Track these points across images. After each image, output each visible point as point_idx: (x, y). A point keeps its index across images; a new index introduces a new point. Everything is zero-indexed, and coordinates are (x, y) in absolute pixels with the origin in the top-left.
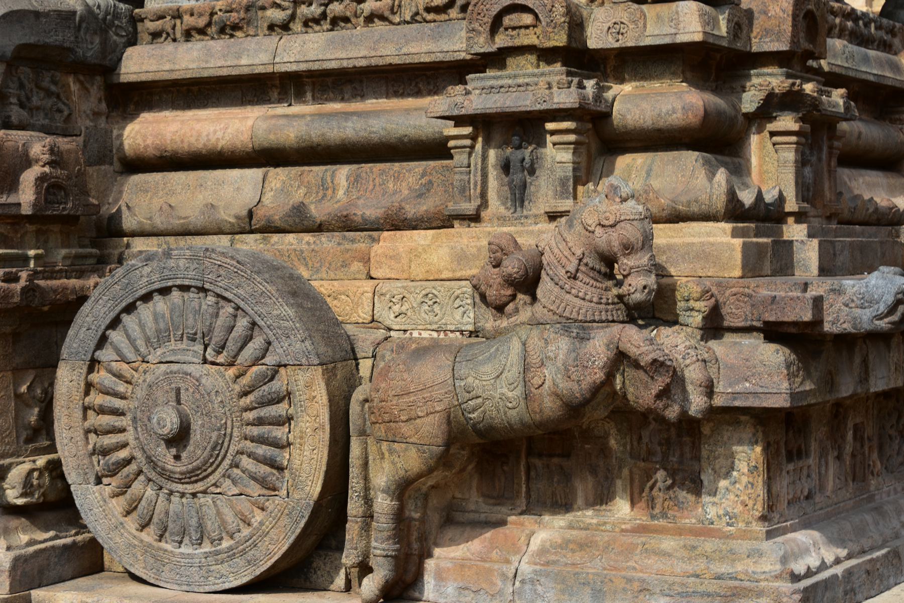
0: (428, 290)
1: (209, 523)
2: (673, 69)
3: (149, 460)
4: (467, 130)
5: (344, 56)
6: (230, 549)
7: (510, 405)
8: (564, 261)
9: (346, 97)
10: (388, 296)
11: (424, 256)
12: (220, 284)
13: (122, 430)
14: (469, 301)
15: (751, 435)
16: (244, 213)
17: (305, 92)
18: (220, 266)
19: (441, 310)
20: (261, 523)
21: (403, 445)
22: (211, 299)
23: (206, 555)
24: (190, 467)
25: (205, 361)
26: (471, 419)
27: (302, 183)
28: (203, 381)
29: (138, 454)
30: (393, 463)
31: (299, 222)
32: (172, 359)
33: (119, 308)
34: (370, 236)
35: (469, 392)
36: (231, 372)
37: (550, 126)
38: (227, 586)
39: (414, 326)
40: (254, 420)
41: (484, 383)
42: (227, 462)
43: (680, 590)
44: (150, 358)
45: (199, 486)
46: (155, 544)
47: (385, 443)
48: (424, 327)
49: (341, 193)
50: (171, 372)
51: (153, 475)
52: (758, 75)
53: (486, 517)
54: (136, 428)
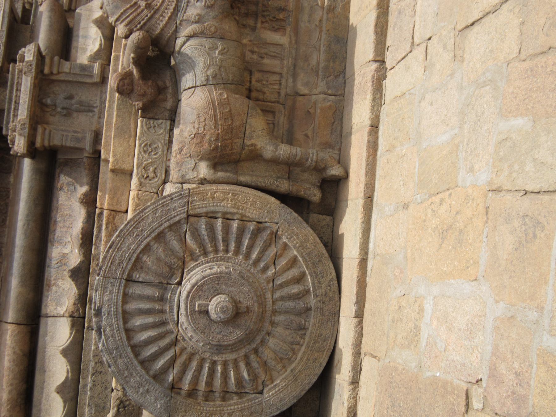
0: (142, 150)
1: (293, 291)
3: (248, 339)
4: (40, 130)
8: (139, 10)
10: (142, 180)
13: (225, 364)
14: (152, 122)
16: (70, 319)
18: (111, 263)
19: (155, 143)
21: (248, 127)
23: (316, 296)
25: (180, 283)
26: (233, 80)
27: (54, 284)
28: (193, 281)
29: (242, 352)
30: (258, 137)
31: (81, 275)
37: (46, 70)
38: (336, 282)
39: (164, 164)
44: (173, 336)
45: (269, 296)
47: (245, 141)
48: (165, 157)
49: (66, 251)
50: (186, 309)
51: (259, 339)
52: (35, 16)
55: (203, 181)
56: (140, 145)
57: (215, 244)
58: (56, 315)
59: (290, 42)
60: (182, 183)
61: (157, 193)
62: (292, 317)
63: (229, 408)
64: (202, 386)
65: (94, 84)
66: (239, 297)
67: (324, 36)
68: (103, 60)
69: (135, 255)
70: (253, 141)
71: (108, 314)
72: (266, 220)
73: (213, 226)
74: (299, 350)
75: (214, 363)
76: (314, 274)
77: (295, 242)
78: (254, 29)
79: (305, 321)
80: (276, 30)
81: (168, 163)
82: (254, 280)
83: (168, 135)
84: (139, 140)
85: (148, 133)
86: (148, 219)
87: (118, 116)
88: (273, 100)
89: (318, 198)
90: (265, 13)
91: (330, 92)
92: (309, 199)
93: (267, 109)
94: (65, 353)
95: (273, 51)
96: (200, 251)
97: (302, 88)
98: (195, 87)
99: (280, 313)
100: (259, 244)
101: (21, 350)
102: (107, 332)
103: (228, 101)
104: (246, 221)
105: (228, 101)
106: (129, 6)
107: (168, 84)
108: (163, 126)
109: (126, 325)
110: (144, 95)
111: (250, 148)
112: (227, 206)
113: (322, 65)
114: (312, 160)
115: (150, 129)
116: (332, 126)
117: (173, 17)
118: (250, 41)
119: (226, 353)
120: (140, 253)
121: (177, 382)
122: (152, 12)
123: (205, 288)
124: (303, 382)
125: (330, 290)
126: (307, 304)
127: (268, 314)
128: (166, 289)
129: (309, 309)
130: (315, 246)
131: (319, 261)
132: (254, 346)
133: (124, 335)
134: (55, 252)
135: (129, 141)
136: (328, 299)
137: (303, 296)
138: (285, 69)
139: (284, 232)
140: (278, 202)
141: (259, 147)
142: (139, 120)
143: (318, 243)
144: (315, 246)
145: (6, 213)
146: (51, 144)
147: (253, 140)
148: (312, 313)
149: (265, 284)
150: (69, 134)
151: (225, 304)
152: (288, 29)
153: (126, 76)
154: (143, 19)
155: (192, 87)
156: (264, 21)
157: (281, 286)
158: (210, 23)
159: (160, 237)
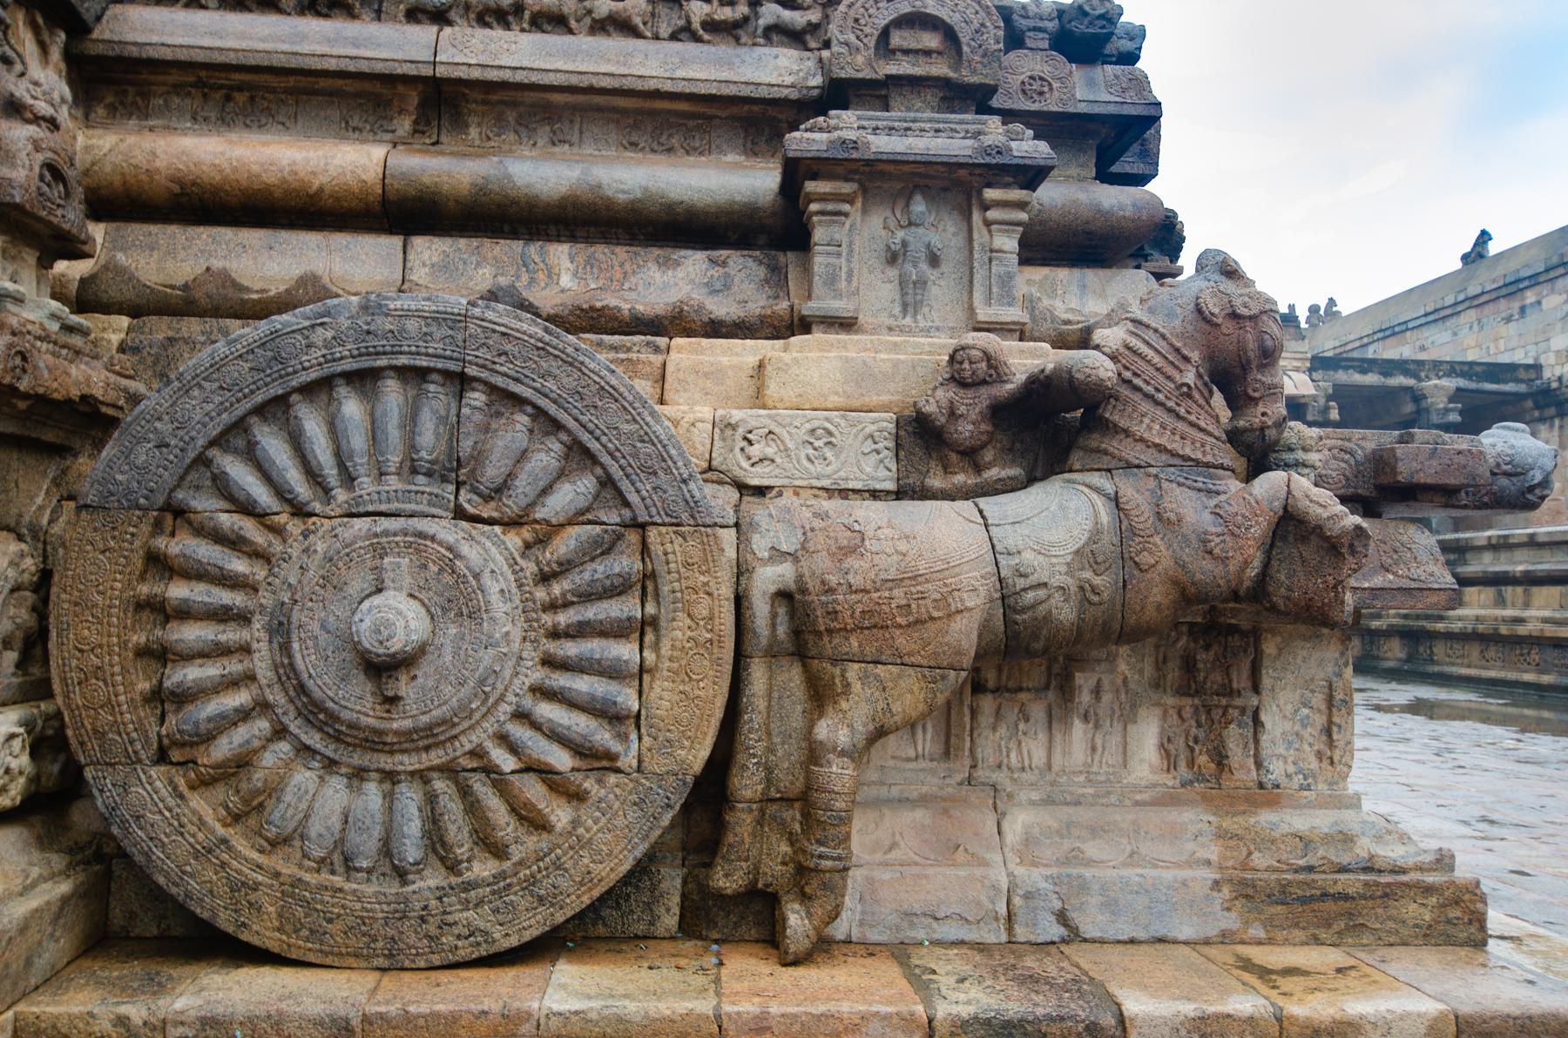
0: (816, 423)
1: (452, 829)
2: (1081, 160)
3: (315, 712)
5: (570, 67)
6: (502, 876)
7: (1096, 599)
9: (540, 143)
11: (795, 370)
12: (503, 369)
13: (246, 650)
15: (1337, 655)
17: (467, 126)
18: (504, 334)
19: (837, 456)
20: (576, 823)
22: (477, 398)
24: (425, 719)
25: (459, 514)
28: (465, 549)
29: (276, 697)
32: (383, 508)
33: (247, 405)
35: (1024, 576)
36: (514, 540)
37: (991, 194)
38: (483, 951)
39: (786, 482)
40: (568, 626)
41: (1054, 560)
42: (505, 709)
43: (1300, 893)
44: (317, 507)
45: (436, 757)
46: (307, 877)
47: (856, 666)
49: (566, 280)
50: (386, 533)
51: (314, 739)
53: (901, 791)
54: (286, 648)
55: (742, 571)
56: (827, 419)
57: (573, 603)
58: (409, 265)
59: (1137, 789)
60: (737, 525)
61: (710, 469)
62: (377, 832)
63: (117, 669)
64: (178, 591)
65: (971, 309)
66: (425, 672)
67: (1168, 875)
69: (525, 392)
70: (857, 687)
71: (368, 332)
72: (646, 739)
73: (620, 594)
74: (287, 859)
75: (244, 618)
76: (502, 884)
77: (590, 822)
79: (369, 871)
80: (1164, 748)
81: (791, 491)
82: (477, 716)
83: (859, 485)
85: (861, 436)
86: (628, 422)
87: (896, 364)
91: (1017, 901)
93: (953, 740)
96: (548, 564)
97: (1018, 827)
99: (389, 797)
100: (579, 723)
101: (321, 190)
102: (320, 330)
103: (959, 612)
104: (641, 685)
105: (959, 612)
106: (1179, 345)
107: (993, 473)
108: (883, 473)
109: (341, 381)
110: (952, 414)
111: (837, 681)
112: (677, 631)
113: (1087, 873)
114: (820, 857)
115: (870, 441)
116: (925, 915)
117: (1164, 457)
118: (1125, 680)
120: (535, 406)
121: (190, 523)
122: (1170, 404)
123: (448, 579)
124: (191, 875)
125: (459, 937)
126: (419, 872)
127: (386, 762)
128: (444, 479)
129: (401, 874)
130: (582, 883)
131: (541, 899)
132: (292, 728)
133: (313, 375)
134: (561, 254)
135: (836, 393)
136: (433, 930)
137: (442, 859)
139: (618, 791)
140: (698, 766)
141: (844, 705)
143: (590, 889)
144: (582, 883)
145: (653, 151)
147: (859, 686)
148: (393, 888)
149: (468, 747)
150: (843, 260)
151: (400, 632)
153: (995, 367)
154: (1148, 383)
155: (983, 517)
157: (465, 792)
158: (1161, 554)
159: (579, 455)
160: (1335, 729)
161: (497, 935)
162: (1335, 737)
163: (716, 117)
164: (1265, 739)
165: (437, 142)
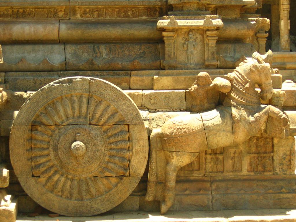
16: (64, 62)
21: (183, 153)
30: (178, 160)
34: (127, 73)
37: (208, 33)
38: (99, 213)
47: (175, 153)
49: (104, 55)
55: (150, 132)
59: (244, 176)
68: (220, 65)
70: (175, 157)
78: (249, 153)
84: (172, 92)
88: (207, 169)
89: (148, 199)
90: (260, 158)
91: (214, 201)
92: (147, 194)
93: (201, 166)
94: (45, 61)
95: (237, 166)
98: (203, 121)
111: (171, 156)
112: (136, 147)
119: (54, 153)
123: (89, 138)
125: (94, 210)
131: (110, 202)
137: (90, 194)
138: (227, 174)
142: (184, 91)
146: (165, 41)
152: (252, 174)
155: (202, 119)
156: (255, 158)
160: (291, 160)
161: (102, 210)
162: (291, 162)
163: (140, 7)
164: (275, 163)
165: (70, 19)
